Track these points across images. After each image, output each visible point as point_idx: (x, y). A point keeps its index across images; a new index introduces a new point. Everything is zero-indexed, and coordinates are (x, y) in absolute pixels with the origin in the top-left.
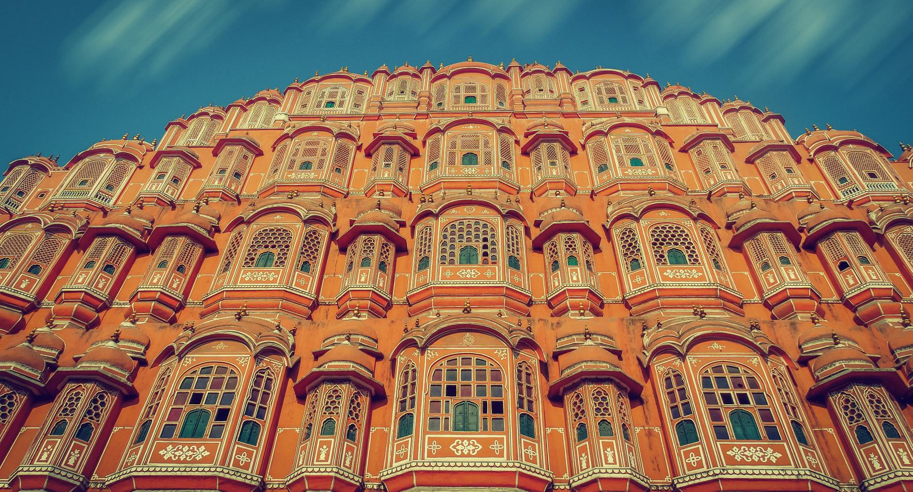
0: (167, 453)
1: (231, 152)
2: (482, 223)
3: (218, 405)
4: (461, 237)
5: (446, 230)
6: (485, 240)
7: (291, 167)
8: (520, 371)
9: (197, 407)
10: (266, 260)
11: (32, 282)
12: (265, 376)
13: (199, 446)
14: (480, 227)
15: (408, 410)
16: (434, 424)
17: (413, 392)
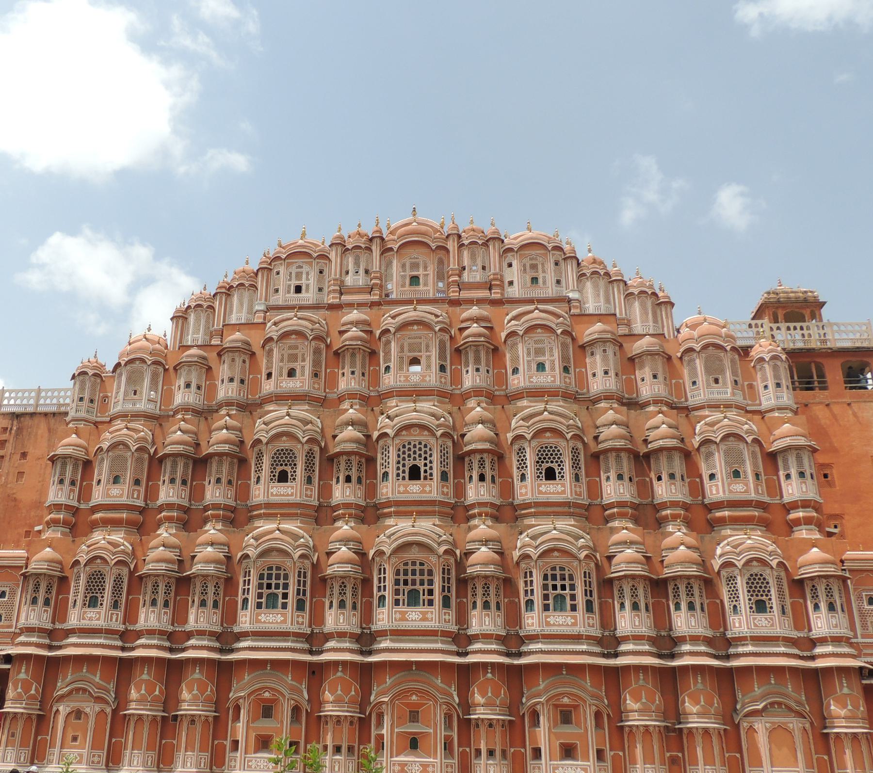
0: (262, 618)
1: (233, 360)
2: (423, 443)
3: (281, 591)
4: (409, 456)
5: (399, 450)
6: (425, 459)
7: (281, 375)
8: (444, 569)
9: (270, 591)
10: (283, 477)
11: (139, 491)
12: (302, 571)
13: (277, 614)
14: (422, 446)
15: (382, 593)
16: (397, 602)
17: (384, 582)
